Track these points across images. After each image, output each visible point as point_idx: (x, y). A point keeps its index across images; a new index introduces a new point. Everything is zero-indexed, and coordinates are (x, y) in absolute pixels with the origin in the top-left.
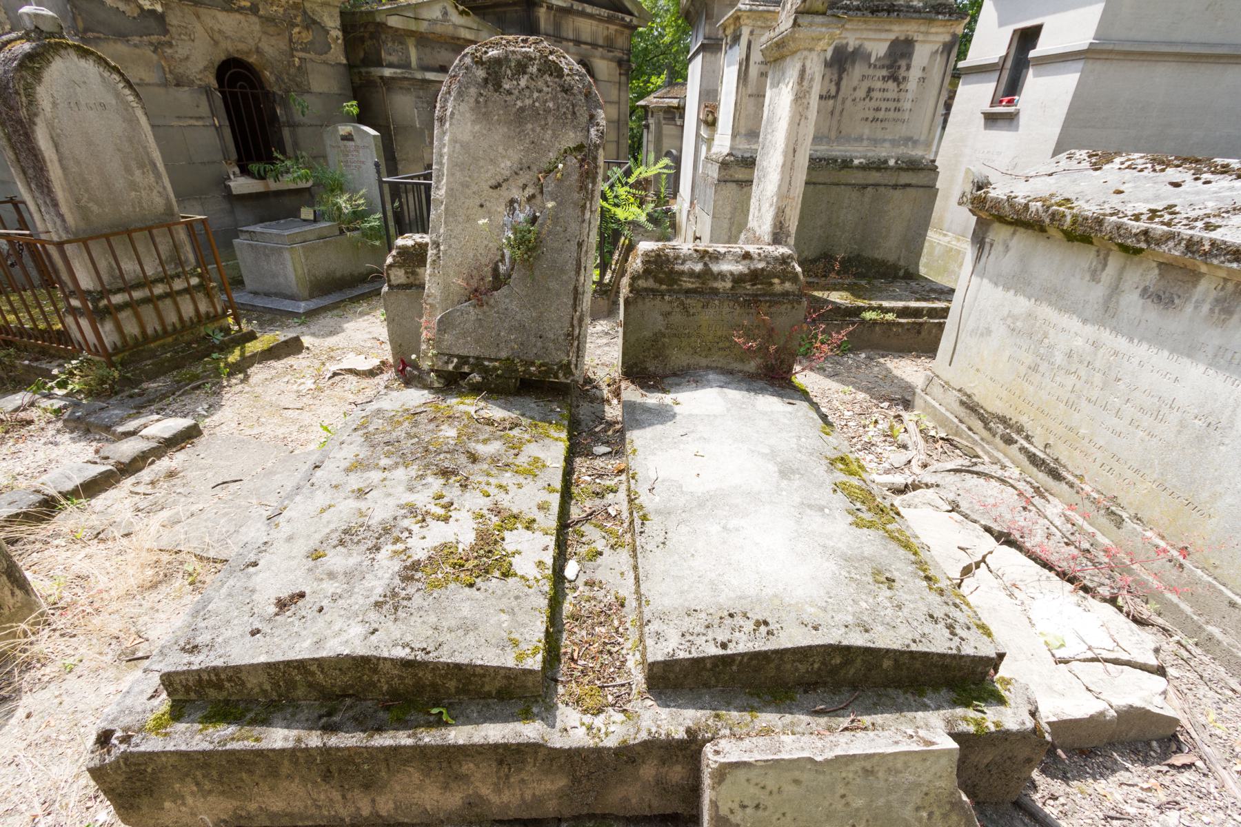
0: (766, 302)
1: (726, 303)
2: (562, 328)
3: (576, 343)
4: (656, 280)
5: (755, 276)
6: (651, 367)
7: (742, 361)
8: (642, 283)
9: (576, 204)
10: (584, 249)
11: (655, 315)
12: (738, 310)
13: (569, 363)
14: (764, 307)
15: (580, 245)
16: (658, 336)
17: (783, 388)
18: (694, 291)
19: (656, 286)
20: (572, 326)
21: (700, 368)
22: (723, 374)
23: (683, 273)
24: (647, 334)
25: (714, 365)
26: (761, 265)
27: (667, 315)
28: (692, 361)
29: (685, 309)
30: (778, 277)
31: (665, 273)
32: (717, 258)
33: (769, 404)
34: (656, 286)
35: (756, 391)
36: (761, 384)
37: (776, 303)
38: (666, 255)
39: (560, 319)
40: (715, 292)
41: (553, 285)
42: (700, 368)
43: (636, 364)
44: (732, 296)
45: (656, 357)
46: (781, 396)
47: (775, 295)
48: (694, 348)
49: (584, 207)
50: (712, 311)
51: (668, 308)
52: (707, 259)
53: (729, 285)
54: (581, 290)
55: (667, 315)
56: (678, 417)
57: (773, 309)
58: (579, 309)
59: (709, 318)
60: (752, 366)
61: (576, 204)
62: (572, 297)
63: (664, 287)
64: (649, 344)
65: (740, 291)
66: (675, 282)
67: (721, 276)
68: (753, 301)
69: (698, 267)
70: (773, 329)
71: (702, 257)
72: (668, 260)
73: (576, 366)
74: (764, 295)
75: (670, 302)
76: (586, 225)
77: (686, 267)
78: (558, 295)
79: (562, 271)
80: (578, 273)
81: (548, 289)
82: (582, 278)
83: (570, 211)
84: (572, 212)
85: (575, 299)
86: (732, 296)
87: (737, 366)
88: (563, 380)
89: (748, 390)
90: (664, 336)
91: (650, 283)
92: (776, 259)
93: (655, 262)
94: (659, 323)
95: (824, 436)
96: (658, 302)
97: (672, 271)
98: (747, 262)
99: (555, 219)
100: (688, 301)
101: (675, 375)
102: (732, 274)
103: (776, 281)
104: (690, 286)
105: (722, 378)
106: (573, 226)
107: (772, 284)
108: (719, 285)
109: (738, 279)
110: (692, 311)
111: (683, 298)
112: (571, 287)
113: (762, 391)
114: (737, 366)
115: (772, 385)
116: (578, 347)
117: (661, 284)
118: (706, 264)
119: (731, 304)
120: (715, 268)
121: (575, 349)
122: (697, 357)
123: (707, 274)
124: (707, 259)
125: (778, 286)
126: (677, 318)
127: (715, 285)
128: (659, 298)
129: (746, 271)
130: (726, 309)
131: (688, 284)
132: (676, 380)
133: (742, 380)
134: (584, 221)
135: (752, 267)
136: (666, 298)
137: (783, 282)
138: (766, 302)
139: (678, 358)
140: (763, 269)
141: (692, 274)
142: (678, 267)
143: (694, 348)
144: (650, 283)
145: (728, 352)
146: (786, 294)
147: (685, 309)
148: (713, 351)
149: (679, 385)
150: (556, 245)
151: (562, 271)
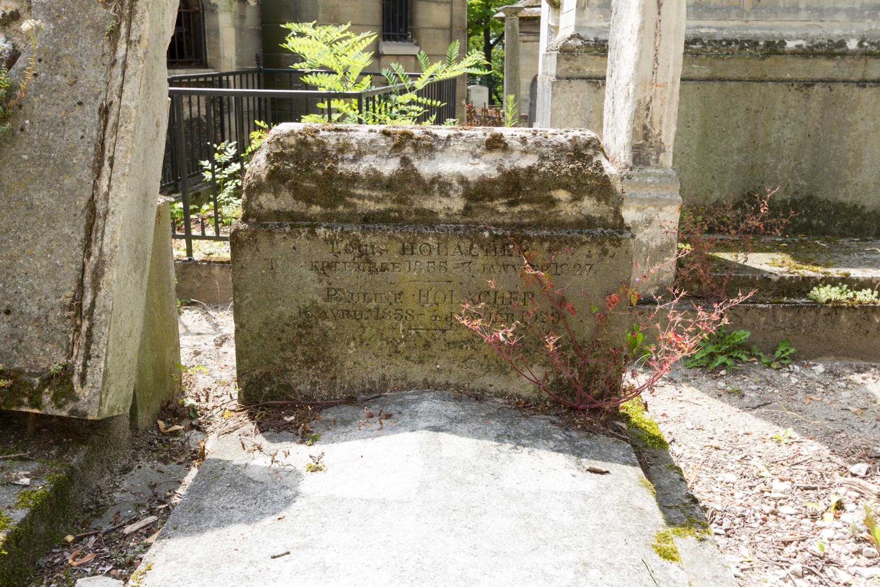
0: (542, 240)
1: (453, 244)
2: (57, 292)
3: (85, 325)
4: (298, 193)
5: (513, 185)
6: (303, 382)
7: (502, 370)
8: (267, 201)
9: (98, 29)
10: (112, 119)
11: (298, 269)
12: (482, 259)
13: (67, 371)
14: (540, 252)
15: (105, 112)
16: (308, 318)
17: (589, 430)
18: (383, 218)
19: (299, 207)
20: (81, 285)
21: (411, 386)
22: (458, 399)
23: (354, 179)
24: (287, 310)
25: (441, 379)
26: (525, 162)
27: (325, 269)
28: (391, 371)
29: (364, 256)
30: (566, 187)
31: (315, 178)
32: (431, 149)
33: (546, 474)
34: (299, 207)
35: (518, 440)
36: (541, 422)
37: (564, 242)
38: (321, 143)
39: (53, 271)
40: (428, 219)
41: (43, 197)
42: (411, 386)
43: (267, 376)
44: (465, 228)
45: (310, 362)
46: (578, 452)
47: (562, 225)
48: (393, 343)
49: (114, 34)
50: (424, 261)
51: (325, 254)
52: (408, 150)
53: (457, 204)
54: (100, 207)
55: (325, 269)
56: (299, 503)
57: (561, 257)
58: (95, 250)
59: (417, 274)
60: (526, 381)
61: (98, 29)
62: (82, 222)
63: (316, 209)
64: (291, 333)
65: (482, 218)
66: (339, 198)
67: (440, 185)
68: (512, 239)
69: (389, 167)
70: (563, 301)
71: (398, 147)
72: (325, 154)
73: (83, 377)
74: (538, 226)
75: (330, 241)
76: (117, 70)
77: (362, 168)
78: (51, 218)
79: (64, 168)
80: (98, 171)
81: (30, 207)
82: (104, 183)
83: (86, 42)
84: (89, 45)
85: (90, 228)
86: (465, 228)
87: (494, 382)
88: (51, 410)
89: (499, 438)
90: (324, 315)
91: (285, 201)
92: (560, 149)
93: (296, 157)
94: (312, 289)
95: (656, 561)
96: (302, 240)
97: (331, 175)
98: (496, 155)
99: (52, 59)
100: (369, 239)
101: (351, 400)
102: (463, 181)
103: (562, 195)
104: (372, 206)
105: (452, 408)
106: (92, 75)
107: (553, 202)
108: (435, 204)
109: (478, 193)
110: (379, 261)
111: (356, 232)
112: (82, 202)
113: (537, 438)
114: (494, 382)
115: (567, 426)
116: (89, 334)
117: (309, 202)
118: (405, 161)
119: (465, 245)
120: (426, 168)
121: (82, 340)
122: (400, 361)
123: (407, 182)
124: (408, 150)
125: (567, 205)
126: (348, 276)
127: (428, 204)
128: (304, 232)
129: (494, 174)
130: (454, 258)
131: (369, 203)
132: (347, 411)
133: (499, 414)
134: (114, 63)
135: (507, 166)
136: (321, 231)
137: (577, 198)
138: (542, 240)
139: (361, 364)
140: (530, 170)
141: (375, 181)
142: (345, 168)
143: (393, 343)
144: (285, 201)
145: (468, 351)
146: (586, 223)
147: (364, 256)
148: (435, 348)
149: (346, 423)
150: (52, 112)
151: (64, 168)
